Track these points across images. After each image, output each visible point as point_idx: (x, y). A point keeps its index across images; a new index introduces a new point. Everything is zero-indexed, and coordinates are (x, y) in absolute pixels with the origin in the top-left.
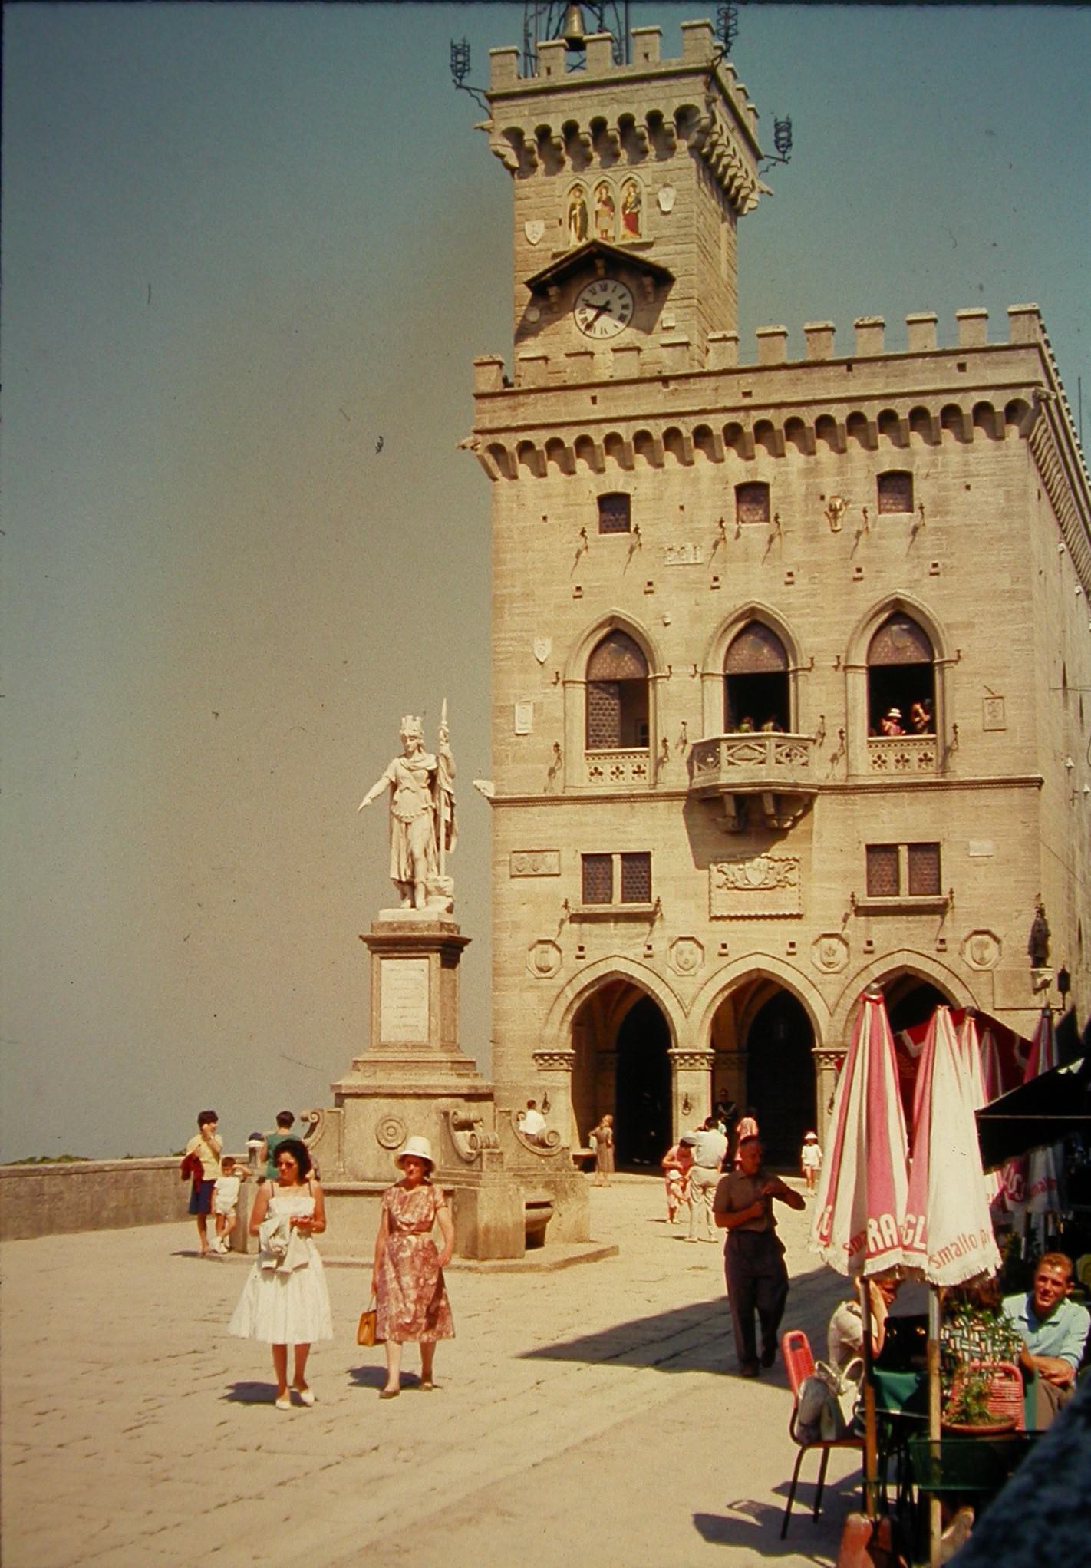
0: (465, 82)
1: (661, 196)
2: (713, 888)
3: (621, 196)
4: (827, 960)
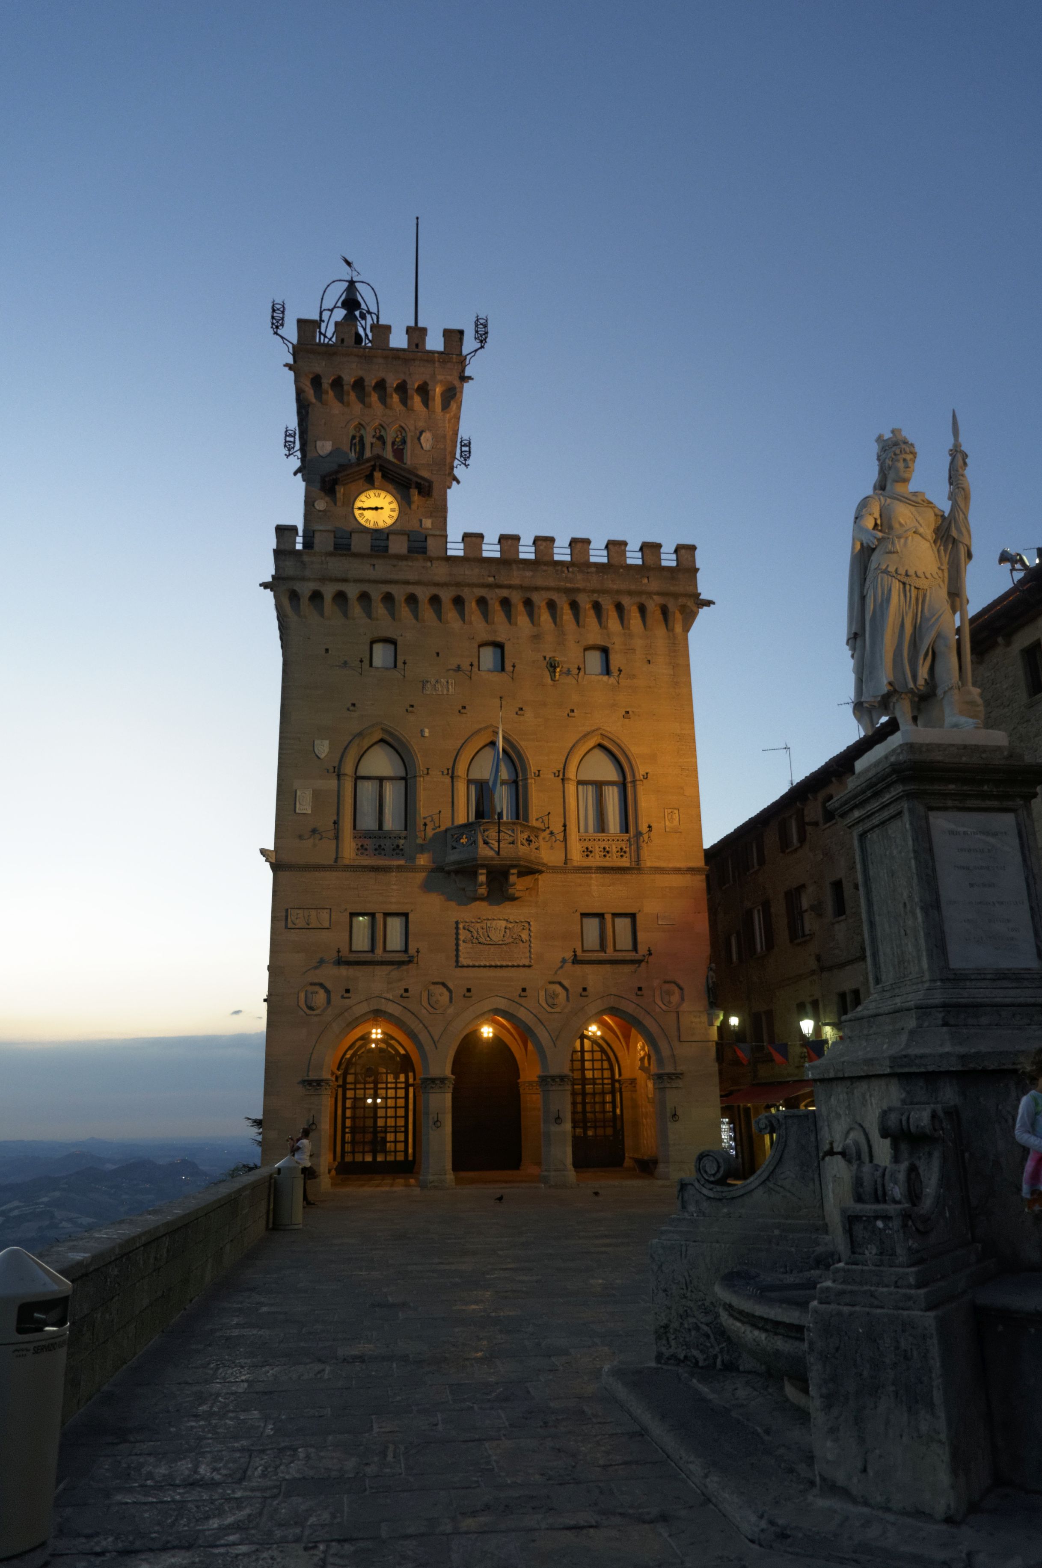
0: (279, 332)
1: (422, 438)
2: (461, 942)
3: (390, 435)
4: (550, 1001)
